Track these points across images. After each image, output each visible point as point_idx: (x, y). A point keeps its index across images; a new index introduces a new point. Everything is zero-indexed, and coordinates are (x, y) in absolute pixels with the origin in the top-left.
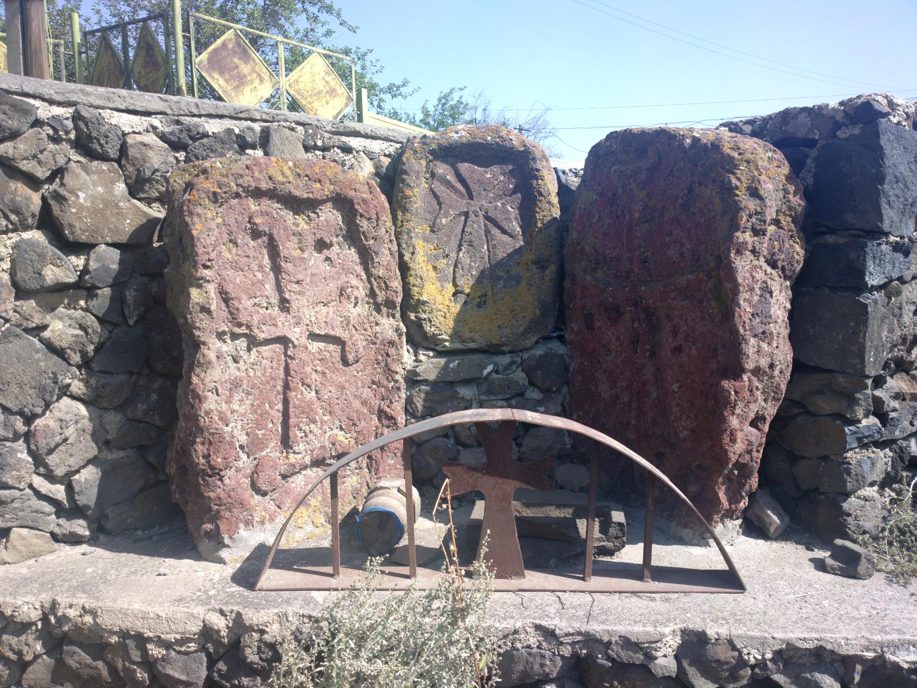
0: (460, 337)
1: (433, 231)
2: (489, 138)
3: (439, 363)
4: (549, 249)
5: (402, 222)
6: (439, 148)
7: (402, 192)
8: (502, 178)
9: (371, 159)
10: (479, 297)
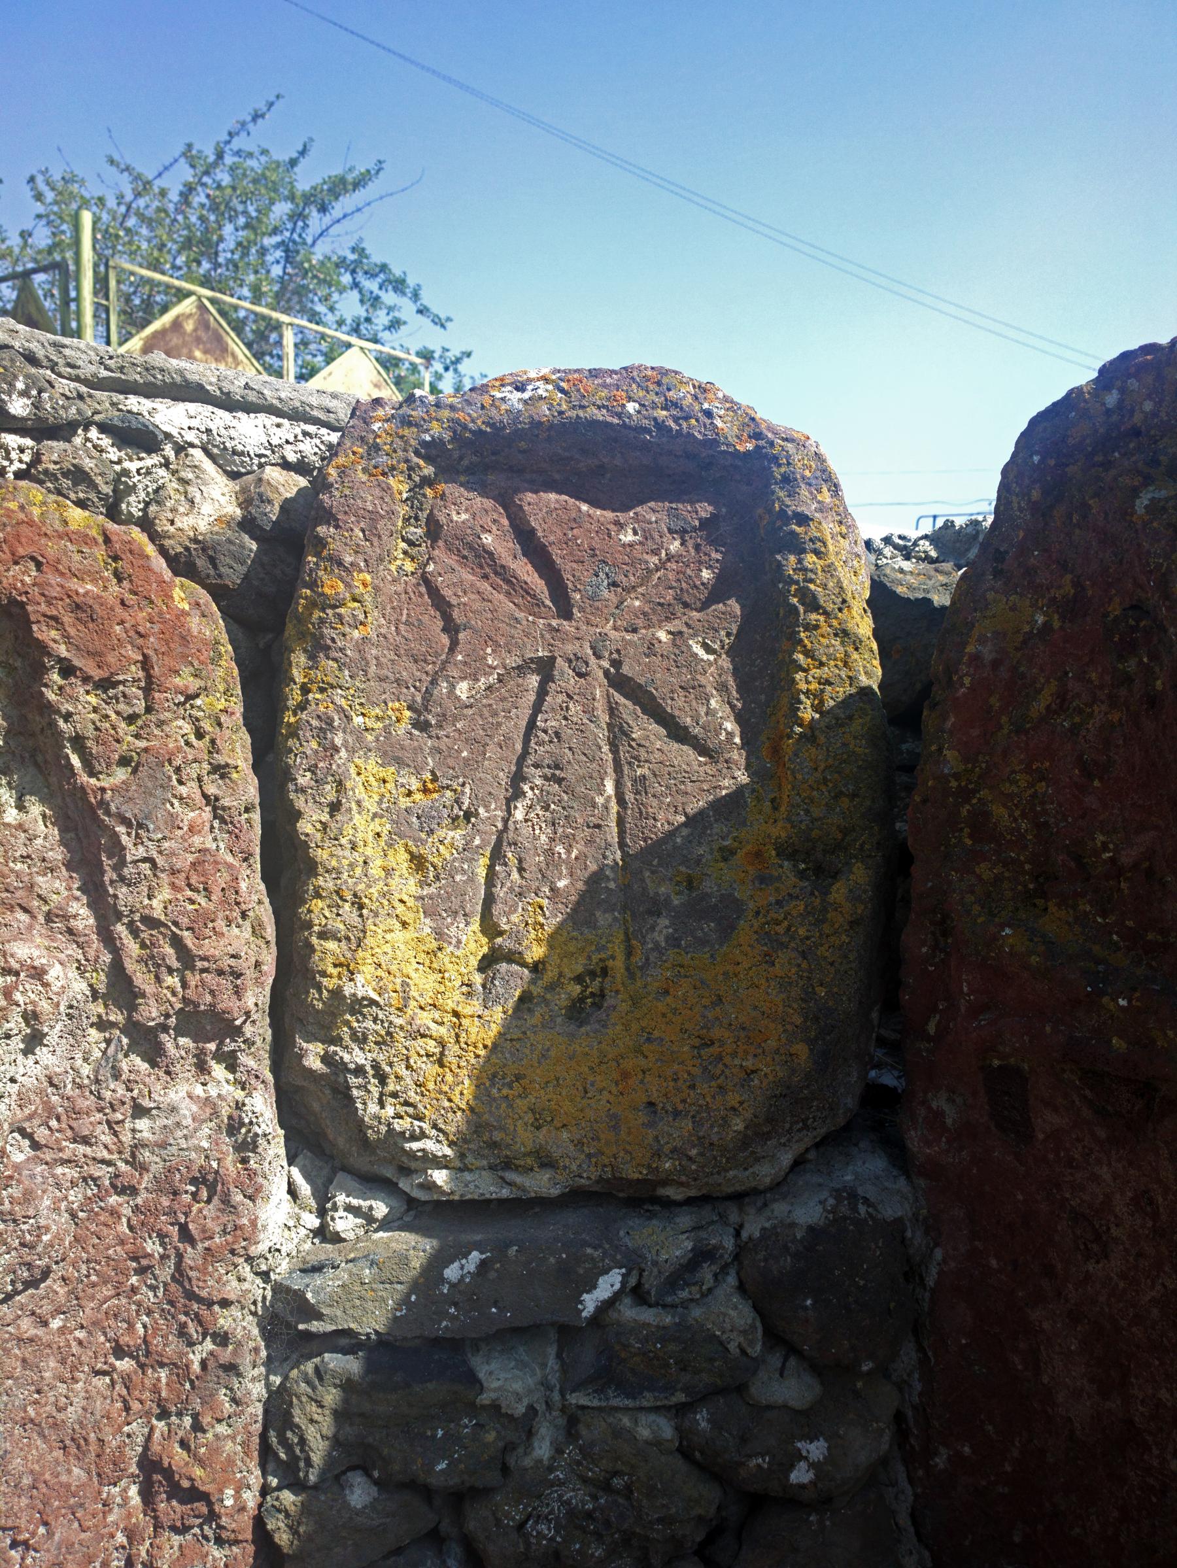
0: (493, 1145)
1: (421, 725)
2: (631, 407)
3: (403, 1260)
4: (845, 802)
5: (305, 690)
6: (455, 438)
7: (313, 585)
8: (675, 546)
9: (234, 476)
10: (579, 979)
